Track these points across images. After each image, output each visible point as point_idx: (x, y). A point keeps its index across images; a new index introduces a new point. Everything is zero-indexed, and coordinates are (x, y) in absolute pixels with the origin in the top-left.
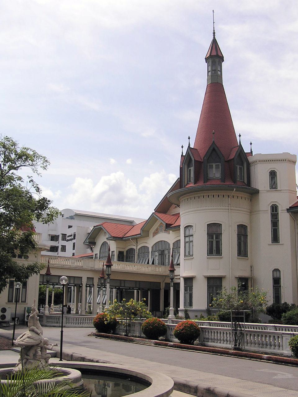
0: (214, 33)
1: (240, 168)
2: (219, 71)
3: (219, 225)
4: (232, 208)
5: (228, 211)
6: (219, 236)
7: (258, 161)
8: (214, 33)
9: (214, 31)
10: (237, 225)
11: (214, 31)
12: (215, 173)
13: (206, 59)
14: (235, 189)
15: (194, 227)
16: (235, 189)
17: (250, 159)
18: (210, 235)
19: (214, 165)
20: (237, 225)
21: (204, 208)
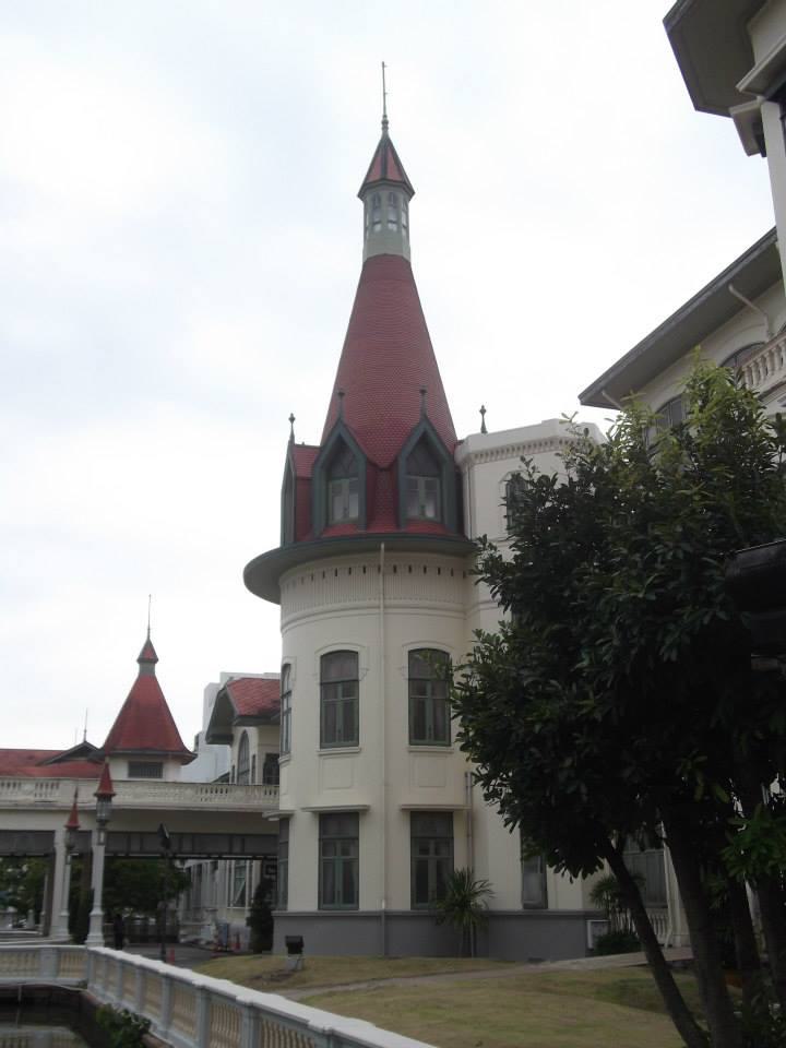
0: (385, 123)
1: (429, 486)
2: (392, 222)
3: (353, 655)
4: (388, 602)
5: (377, 611)
6: (351, 687)
7: (473, 457)
8: (385, 123)
9: (385, 116)
10: (411, 652)
11: (385, 116)
12: (348, 507)
13: (361, 195)
14: (383, 546)
15: (293, 667)
16: (383, 546)
17: (460, 455)
18: (326, 686)
19: (345, 483)
20: (411, 652)
21: (320, 608)
